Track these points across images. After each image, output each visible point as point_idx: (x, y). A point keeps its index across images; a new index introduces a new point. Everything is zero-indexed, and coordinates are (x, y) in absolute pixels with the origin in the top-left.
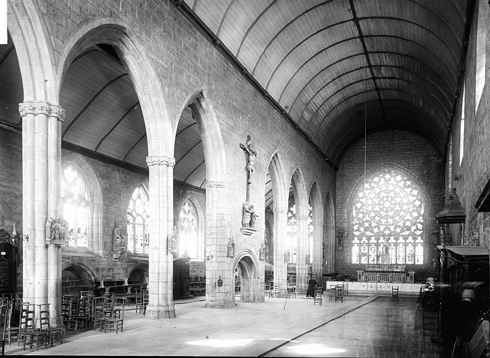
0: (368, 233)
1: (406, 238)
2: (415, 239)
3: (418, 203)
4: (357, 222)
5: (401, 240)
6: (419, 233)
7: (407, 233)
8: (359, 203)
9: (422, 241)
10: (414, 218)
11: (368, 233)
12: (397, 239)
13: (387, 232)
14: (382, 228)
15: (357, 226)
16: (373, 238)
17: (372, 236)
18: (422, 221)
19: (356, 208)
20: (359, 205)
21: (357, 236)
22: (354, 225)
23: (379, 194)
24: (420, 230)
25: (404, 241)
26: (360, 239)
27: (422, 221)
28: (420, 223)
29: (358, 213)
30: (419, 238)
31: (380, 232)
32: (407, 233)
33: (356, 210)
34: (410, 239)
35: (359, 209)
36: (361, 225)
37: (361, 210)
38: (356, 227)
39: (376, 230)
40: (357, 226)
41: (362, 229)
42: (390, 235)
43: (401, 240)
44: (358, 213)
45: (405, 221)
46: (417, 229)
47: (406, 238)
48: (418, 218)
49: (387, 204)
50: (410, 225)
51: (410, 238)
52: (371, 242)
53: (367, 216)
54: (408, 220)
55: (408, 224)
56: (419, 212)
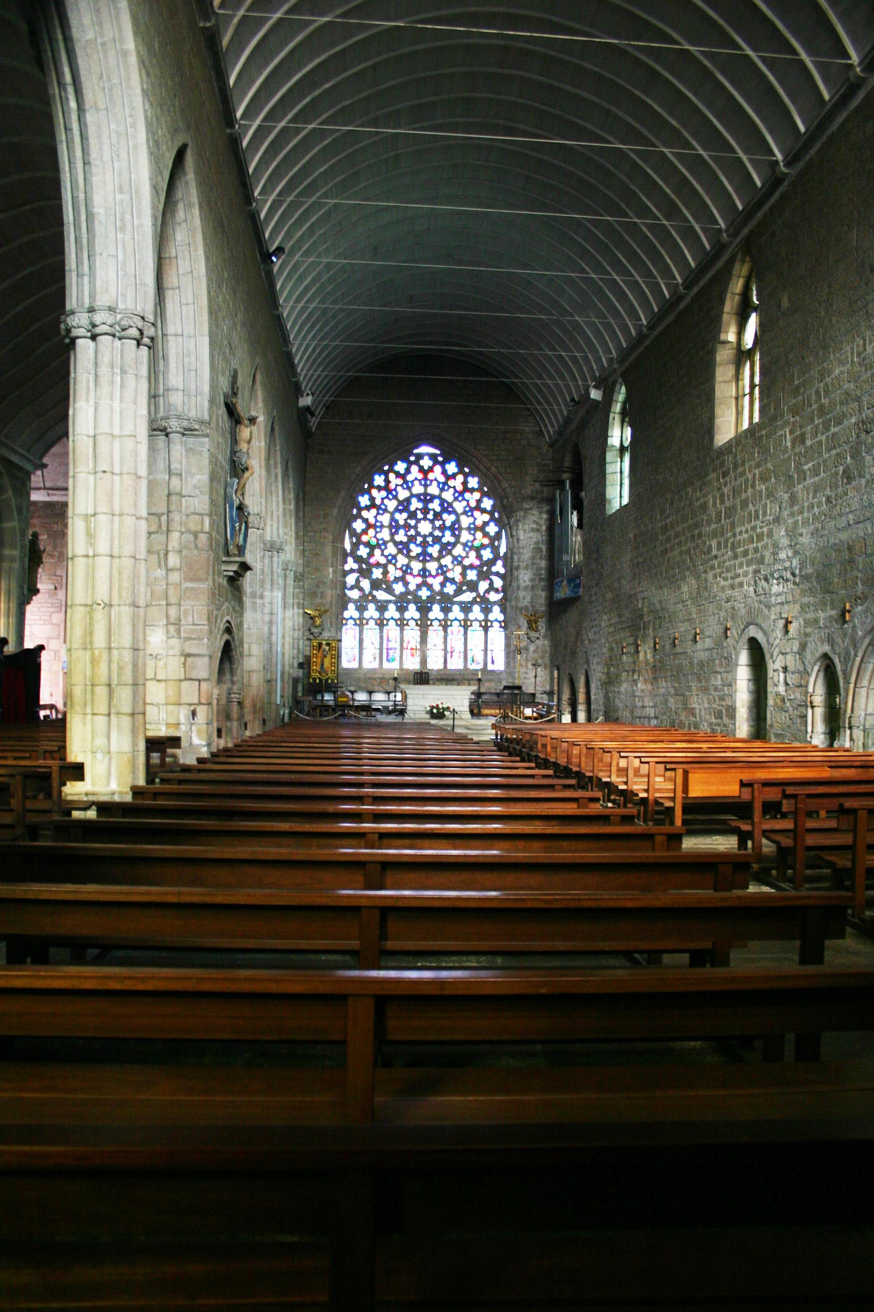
0: (381, 595)
1: (466, 608)
2: (486, 611)
3: (492, 529)
6: (494, 597)
7: (467, 597)
9: (501, 617)
11: (381, 595)
12: (446, 610)
13: (424, 593)
14: (413, 582)
15: (355, 575)
16: (392, 607)
17: (389, 602)
18: (502, 571)
19: (353, 533)
20: (359, 526)
21: (355, 602)
22: (345, 574)
23: (408, 501)
24: (497, 591)
25: (461, 616)
26: (361, 609)
27: (502, 571)
28: (497, 574)
29: (355, 546)
30: (496, 609)
31: (408, 592)
32: (467, 597)
33: (351, 538)
34: (476, 613)
35: (358, 536)
36: (365, 573)
37: (364, 538)
38: (351, 580)
39: (399, 588)
40: (355, 575)
41: (365, 584)
42: (431, 600)
43: (456, 612)
44: (355, 546)
45: (465, 568)
46: (491, 588)
47: (466, 608)
48: (492, 562)
49: (425, 528)
50: (475, 578)
51: (476, 608)
52: (387, 615)
53: (377, 552)
54: (472, 567)
55: (472, 575)
56: (495, 550)
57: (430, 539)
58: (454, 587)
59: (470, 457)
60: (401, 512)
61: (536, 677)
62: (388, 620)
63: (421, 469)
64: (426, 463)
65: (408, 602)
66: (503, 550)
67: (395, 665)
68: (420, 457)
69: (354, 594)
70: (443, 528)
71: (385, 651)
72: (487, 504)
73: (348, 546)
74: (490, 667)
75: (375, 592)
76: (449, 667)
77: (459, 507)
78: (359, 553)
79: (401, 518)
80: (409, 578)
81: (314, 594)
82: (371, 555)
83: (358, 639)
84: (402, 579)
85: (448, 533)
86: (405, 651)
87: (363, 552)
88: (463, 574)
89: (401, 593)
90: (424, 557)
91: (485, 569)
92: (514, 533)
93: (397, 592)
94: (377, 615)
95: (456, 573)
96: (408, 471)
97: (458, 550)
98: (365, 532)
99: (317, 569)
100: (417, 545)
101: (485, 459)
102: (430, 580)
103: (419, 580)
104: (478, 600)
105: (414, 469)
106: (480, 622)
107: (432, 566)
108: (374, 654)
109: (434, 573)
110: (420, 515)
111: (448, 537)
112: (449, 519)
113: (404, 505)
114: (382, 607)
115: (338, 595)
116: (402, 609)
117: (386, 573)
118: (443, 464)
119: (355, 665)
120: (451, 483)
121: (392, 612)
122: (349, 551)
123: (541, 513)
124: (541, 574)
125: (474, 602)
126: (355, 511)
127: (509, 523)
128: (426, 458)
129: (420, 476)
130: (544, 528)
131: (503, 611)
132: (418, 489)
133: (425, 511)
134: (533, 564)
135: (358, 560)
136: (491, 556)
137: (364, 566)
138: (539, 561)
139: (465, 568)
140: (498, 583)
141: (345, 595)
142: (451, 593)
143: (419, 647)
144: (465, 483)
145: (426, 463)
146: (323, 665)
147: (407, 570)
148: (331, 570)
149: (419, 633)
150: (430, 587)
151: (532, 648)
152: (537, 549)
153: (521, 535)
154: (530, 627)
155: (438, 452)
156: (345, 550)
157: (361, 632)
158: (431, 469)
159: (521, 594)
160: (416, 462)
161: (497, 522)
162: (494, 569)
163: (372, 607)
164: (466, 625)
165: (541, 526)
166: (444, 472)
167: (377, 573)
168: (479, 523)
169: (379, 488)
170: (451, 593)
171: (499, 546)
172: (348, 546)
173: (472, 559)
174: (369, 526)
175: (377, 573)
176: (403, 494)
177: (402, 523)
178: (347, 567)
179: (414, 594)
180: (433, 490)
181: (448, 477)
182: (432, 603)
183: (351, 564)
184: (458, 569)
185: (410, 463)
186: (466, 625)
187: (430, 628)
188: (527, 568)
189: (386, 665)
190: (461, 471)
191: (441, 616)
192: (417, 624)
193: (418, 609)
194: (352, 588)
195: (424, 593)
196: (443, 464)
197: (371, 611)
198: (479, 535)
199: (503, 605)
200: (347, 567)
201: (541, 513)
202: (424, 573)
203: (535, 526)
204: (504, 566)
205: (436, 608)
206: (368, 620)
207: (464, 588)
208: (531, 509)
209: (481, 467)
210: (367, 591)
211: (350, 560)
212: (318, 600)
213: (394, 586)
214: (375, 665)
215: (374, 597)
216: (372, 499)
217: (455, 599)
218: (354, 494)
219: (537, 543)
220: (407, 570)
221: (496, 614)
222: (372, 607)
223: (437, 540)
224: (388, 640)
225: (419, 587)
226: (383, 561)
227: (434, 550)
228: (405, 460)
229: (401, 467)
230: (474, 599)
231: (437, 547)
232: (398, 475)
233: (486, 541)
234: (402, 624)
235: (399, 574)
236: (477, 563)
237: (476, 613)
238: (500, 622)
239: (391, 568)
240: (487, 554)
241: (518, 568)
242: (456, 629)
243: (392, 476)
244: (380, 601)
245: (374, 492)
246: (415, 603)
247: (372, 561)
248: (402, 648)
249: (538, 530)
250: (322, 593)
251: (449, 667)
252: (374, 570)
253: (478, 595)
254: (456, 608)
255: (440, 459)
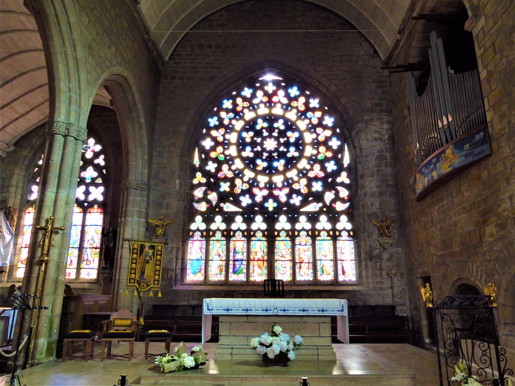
0: (229, 207)
1: (313, 218)
3: (335, 143)
4: (204, 180)
5: (303, 223)
7: (313, 207)
8: (208, 140)
9: (349, 226)
10: (328, 175)
11: (229, 207)
12: (293, 220)
13: (271, 205)
14: (260, 195)
15: (204, 188)
16: (239, 219)
17: (236, 213)
18: (347, 181)
19: (202, 150)
20: (207, 143)
21: (202, 214)
22: (194, 187)
24: (343, 201)
25: (308, 226)
26: (208, 219)
27: (347, 181)
28: (342, 184)
29: (204, 162)
30: (344, 218)
31: (254, 204)
32: (313, 207)
33: (200, 154)
34: (323, 223)
35: (207, 153)
37: (213, 155)
38: (198, 193)
39: (246, 201)
40: (204, 188)
41: (213, 197)
42: (278, 211)
43: (303, 223)
44: (204, 162)
46: (337, 198)
47: (313, 218)
48: (336, 174)
49: (270, 144)
51: (323, 218)
52: (234, 227)
53: (225, 167)
55: (317, 187)
57: (275, 154)
58: (300, 198)
59: (310, 80)
60: (247, 131)
61: (392, 288)
62: (235, 232)
63: (266, 94)
64: (270, 88)
65: (255, 213)
66: (346, 161)
67: (242, 277)
68: (264, 83)
69: (203, 207)
70: (287, 144)
71: (231, 263)
72: (329, 121)
73: (197, 162)
74: (341, 278)
75: (222, 205)
76: (299, 278)
77: (302, 125)
78: (207, 168)
79: (248, 136)
80: (255, 190)
81: (159, 205)
82: (219, 169)
83: (204, 251)
84: (249, 192)
85: (292, 149)
86: (252, 263)
87: (211, 167)
88: (309, 186)
89: (248, 205)
90: (270, 171)
91: (330, 180)
92: (357, 144)
93: (244, 204)
94: (223, 226)
95: (302, 185)
96: (254, 96)
97: (303, 164)
98: (213, 149)
99: (164, 181)
100: (263, 160)
101: (324, 79)
102: (276, 192)
103: (265, 192)
104: (325, 209)
105: (260, 94)
106: (328, 232)
107: (278, 180)
108: (220, 266)
109: (280, 185)
110: (265, 134)
111: (292, 152)
112: (293, 136)
113: (251, 126)
114: (229, 218)
115: (185, 207)
116: (249, 221)
117: (233, 186)
118: (285, 88)
119: (200, 277)
120: (294, 104)
121: (239, 223)
122: (197, 166)
123: (382, 123)
124: (388, 181)
125: (320, 212)
126: (204, 131)
127: (350, 136)
128: (271, 84)
129: (265, 99)
130: (386, 137)
131: (351, 219)
132: (263, 110)
133: (271, 129)
134: (378, 171)
135: (207, 174)
136: (335, 168)
137: (212, 180)
138: (384, 168)
139: (310, 181)
140: (344, 193)
141: (192, 207)
142: (298, 204)
143: (266, 258)
144: (307, 104)
145: (270, 88)
146: (143, 273)
147: (253, 183)
148: (178, 182)
149: (265, 243)
150: (276, 199)
151: (385, 256)
152: (381, 157)
153: (364, 144)
154: (381, 235)
155: (281, 79)
156: (195, 165)
157: (208, 245)
158: (275, 93)
159: (369, 200)
160: (261, 88)
161: (339, 137)
162: (339, 180)
163: (218, 219)
164: (314, 235)
165: (383, 135)
166: (287, 95)
167: (225, 187)
168: (321, 138)
169: (227, 111)
170: (298, 204)
171: (342, 159)
172: (197, 162)
173: (317, 171)
174: (217, 143)
175: (225, 187)
176: (249, 115)
177: (248, 140)
178: (195, 182)
179: (261, 205)
180: (278, 111)
181: (291, 99)
182: (279, 214)
183: (199, 178)
184: (304, 181)
185: (255, 89)
186: (314, 235)
187: (278, 239)
188: (372, 175)
189: (233, 277)
190: (302, 94)
191: (288, 226)
192: (264, 235)
193: (265, 220)
194: (199, 201)
195: (271, 205)
196: (285, 88)
197: (218, 223)
198: (322, 149)
199: (350, 213)
200: (195, 182)
201: (382, 123)
202: (270, 186)
203: (377, 136)
204: (348, 177)
205: (283, 218)
206: (214, 232)
207: (311, 199)
208: (372, 120)
209: (321, 88)
210: (214, 203)
211: (199, 175)
212: (164, 211)
213: (242, 198)
214: (222, 278)
215: (221, 209)
216: (221, 120)
217: (301, 210)
218: (204, 116)
219: (380, 151)
220: (253, 183)
221: (344, 223)
222: (218, 219)
223: (282, 155)
224: (235, 252)
225: (265, 199)
226: (230, 175)
227: (280, 164)
228: (251, 85)
229: (247, 92)
230: (321, 209)
231: (282, 162)
232: (245, 99)
233: (329, 154)
234: (249, 235)
235: (246, 186)
236: (322, 174)
237: (323, 223)
238: (349, 231)
239: (238, 182)
240: (331, 166)
241: (362, 177)
242: (303, 239)
243: (239, 101)
244: (227, 213)
245: (223, 114)
246: (262, 214)
247: (220, 175)
248: (249, 260)
249: (380, 139)
250: (168, 204)
251: (299, 278)
252: (222, 184)
253: (325, 205)
254: (303, 219)
255: (283, 84)
